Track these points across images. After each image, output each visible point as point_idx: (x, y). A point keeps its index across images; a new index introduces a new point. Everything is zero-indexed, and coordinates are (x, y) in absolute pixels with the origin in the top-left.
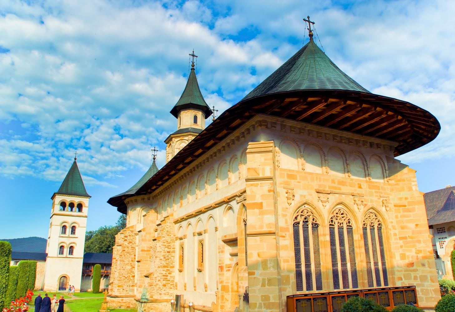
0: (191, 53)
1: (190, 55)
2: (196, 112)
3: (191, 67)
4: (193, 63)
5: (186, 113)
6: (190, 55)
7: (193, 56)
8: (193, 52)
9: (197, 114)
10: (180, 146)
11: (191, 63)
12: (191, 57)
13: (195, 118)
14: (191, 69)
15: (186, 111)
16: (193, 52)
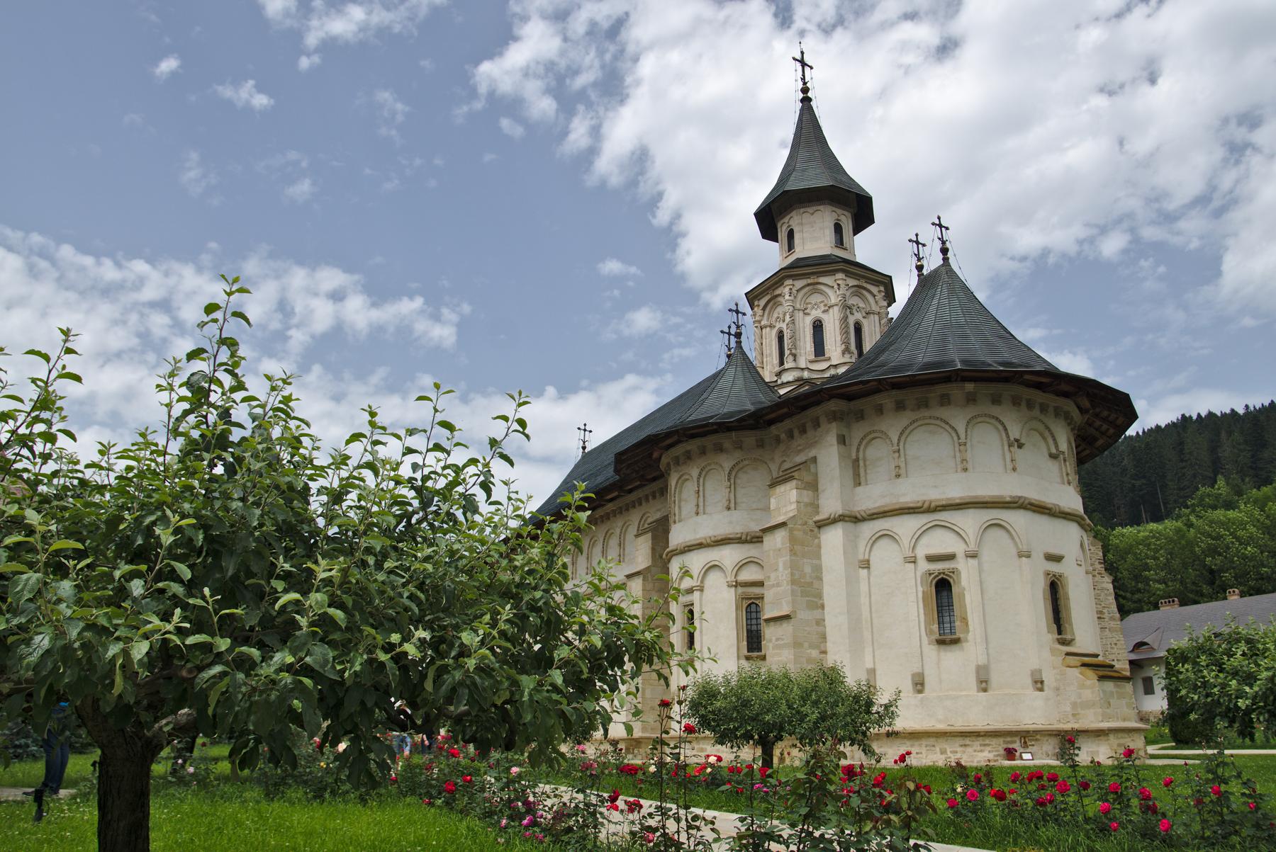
0: (799, 57)
1: (794, 59)
2: (839, 211)
3: (801, 96)
4: (805, 83)
5: (812, 214)
6: (794, 59)
7: (803, 64)
8: (802, 53)
9: (843, 218)
10: (807, 301)
11: (800, 85)
12: (799, 65)
13: (838, 229)
14: (802, 101)
15: (810, 210)
16: (802, 53)
